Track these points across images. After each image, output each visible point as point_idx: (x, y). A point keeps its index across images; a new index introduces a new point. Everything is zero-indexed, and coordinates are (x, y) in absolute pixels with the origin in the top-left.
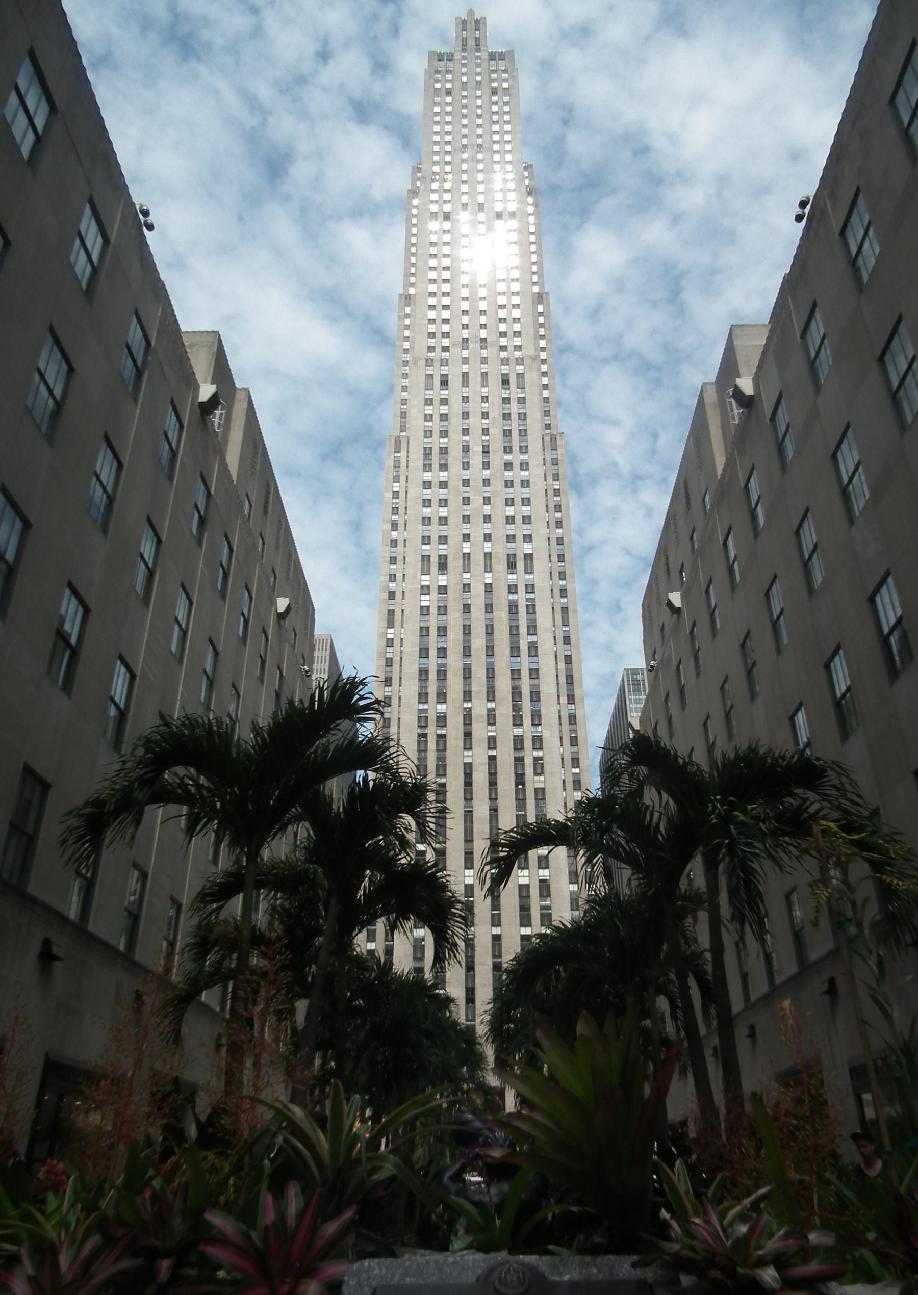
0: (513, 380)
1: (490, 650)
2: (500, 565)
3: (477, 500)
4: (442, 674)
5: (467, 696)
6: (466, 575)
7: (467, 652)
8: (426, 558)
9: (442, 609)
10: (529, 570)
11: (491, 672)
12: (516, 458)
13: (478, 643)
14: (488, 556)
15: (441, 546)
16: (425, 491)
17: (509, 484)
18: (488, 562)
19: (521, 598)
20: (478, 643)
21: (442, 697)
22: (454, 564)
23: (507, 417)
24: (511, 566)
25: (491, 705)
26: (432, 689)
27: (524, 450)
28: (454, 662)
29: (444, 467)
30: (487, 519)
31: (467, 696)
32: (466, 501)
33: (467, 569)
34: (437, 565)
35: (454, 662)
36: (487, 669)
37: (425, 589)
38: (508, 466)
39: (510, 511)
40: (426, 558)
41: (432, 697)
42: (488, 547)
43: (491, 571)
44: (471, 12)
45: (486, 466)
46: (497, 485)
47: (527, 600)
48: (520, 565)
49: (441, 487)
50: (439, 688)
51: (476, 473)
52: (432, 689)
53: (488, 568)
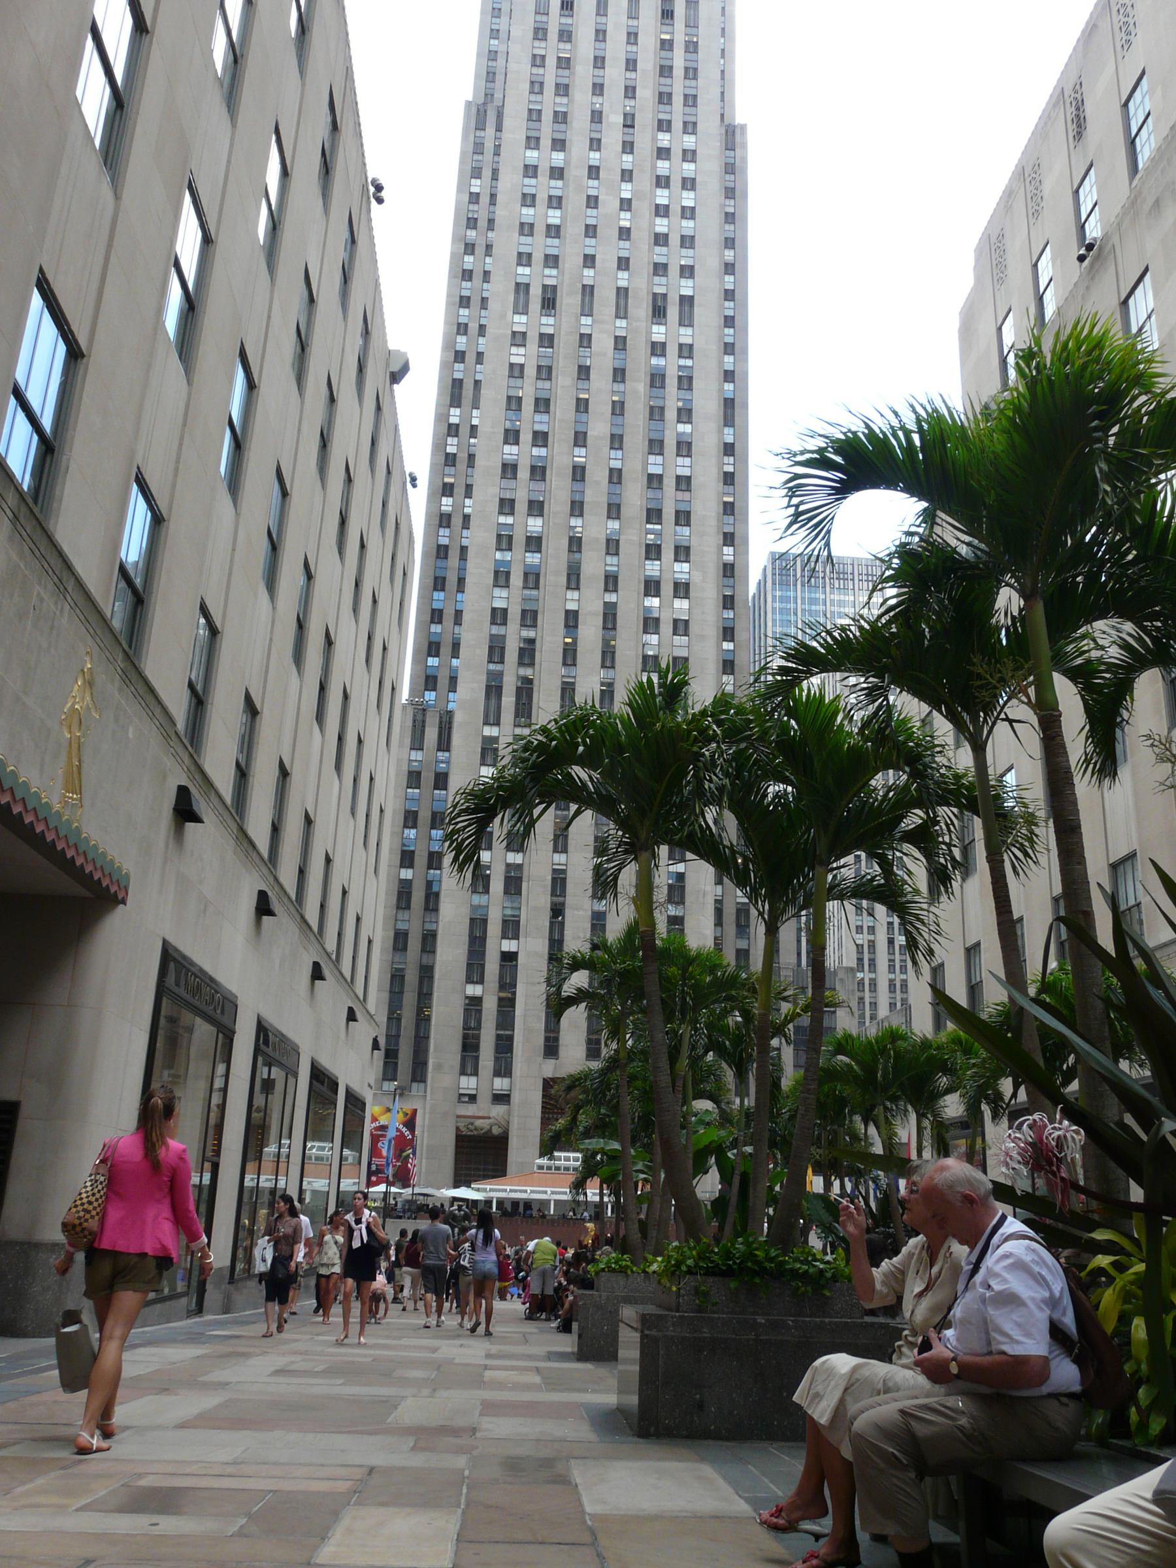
2: (640, 309)
3: (609, 203)
5: (577, 508)
8: (522, 289)
10: (686, 319)
14: (622, 293)
15: (547, 271)
16: (527, 181)
18: (622, 302)
19: (671, 364)
22: (569, 301)
24: (658, 311)
29: (559, 144)
30: (624, 234)
31: (577, 508)
32: (592, 202)
34: (539, 301)
38: (663, 153)
39: (661, 225)
40: (522, 289)
42: (623, 279)
43: (625, 318)
45: (628, 147)
48: (673, 312)
49: (552, 177)
51: (611, 157)
53: (621, 311)
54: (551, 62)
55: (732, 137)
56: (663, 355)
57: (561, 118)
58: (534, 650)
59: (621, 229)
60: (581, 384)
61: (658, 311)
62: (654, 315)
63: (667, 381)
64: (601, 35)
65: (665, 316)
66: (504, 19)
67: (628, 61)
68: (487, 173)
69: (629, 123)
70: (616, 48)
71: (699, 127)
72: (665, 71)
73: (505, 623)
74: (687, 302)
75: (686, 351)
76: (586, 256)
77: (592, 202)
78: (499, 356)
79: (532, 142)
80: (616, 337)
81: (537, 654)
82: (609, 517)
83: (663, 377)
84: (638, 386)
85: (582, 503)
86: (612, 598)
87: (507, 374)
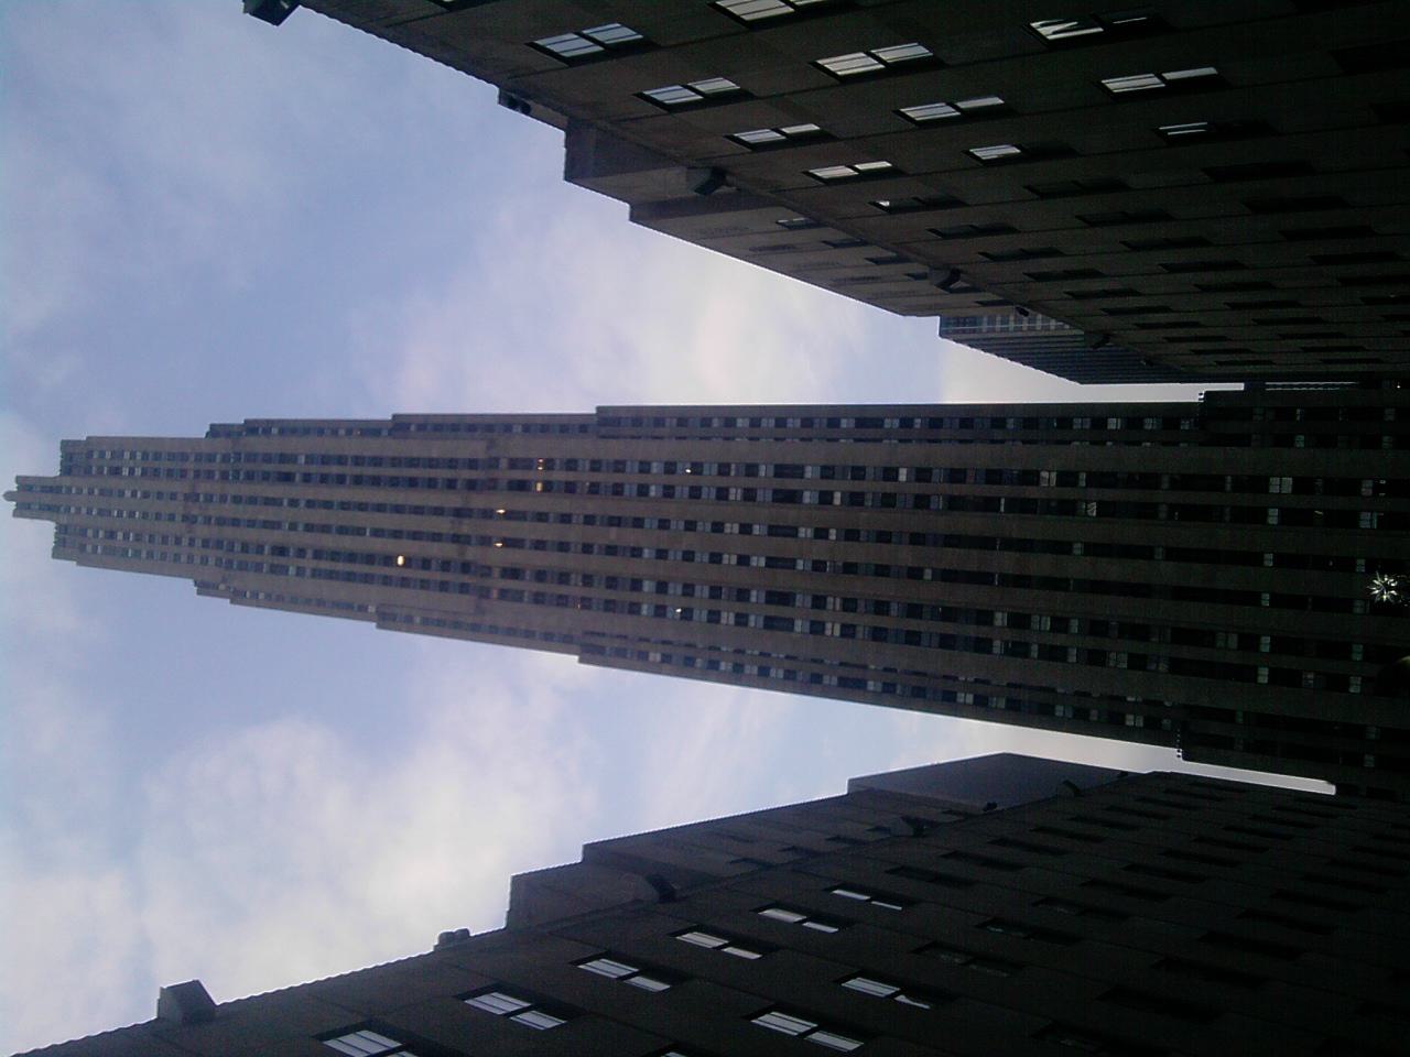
0: (518, 475)
2: (789, 514)
3: (689, 541)
6: (800, 565)
12: (631, 479)
14: (774, 531)
15: (830, 607)
17: (668, 492)
22: (781, 580)
23: (594, 489)
24: (791, 497)
26: (972, 630)
27: (619, 466)
33: (789, 564)
34: (781, 608)
38: (643, 491)
40: (770, 623)
41: (983, 631)
44: (9, 496)
45: (638, 523)
46: (670, 509)
47: (844, 478)
48: (791, 484)
52: (972, 630)
53: (791, 532)
57: (612, 582)
61: (791, 497)
63: (857, 490)
64: (540, 545)
65: (795, 492)
68: (643, 646)
69: (616, 522)
72: (570, 488)
74: (781, 471)
75: (827, 472)
77: (688, 556)
79: (634, 609)
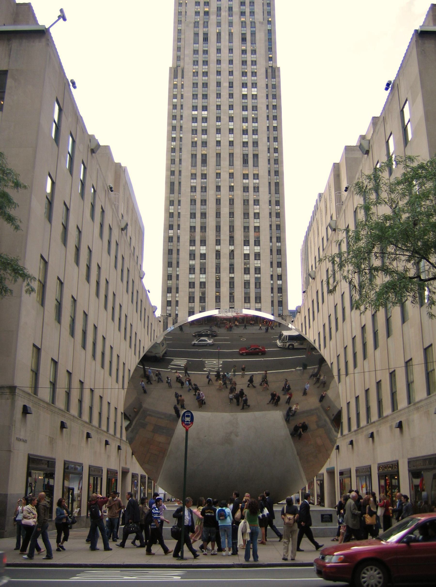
1: (232, 214)
4: (203, 228)
5: (218, 242)
7: (218, 215)
9: (204, 189)
10: (256, 164)
11: (232, 228)
13: (225, 210)
20: (225, 210)
21: (203, 242)
24: (245, 161)
25: (232, 248)
28: (211, 222)
30: (231, 131)
31: (218, 242)
34: (200, 161)
35: (211, 222)
36: (230, 226)
37: (194, 176)
40: (194, 156)
41: (198, 242)
50: (201, 237)
54: (201, 52)
55: (273, 72)
56: (248, 179)
58: (205, 297)
59: (230, 129)
60: (218, 193)
62: (243, 163)
66: (182, 61)
67: (229, 61)
69: (231, 85)
70: (225, 55)
71: (258, 85)
73: (194, 288)
76: (217, 105)
78: (187, 183)
80: (230, 173)
81: (206, 299)
82: (230, 245)
83: (248, 188)
84: (238, 194)
85: (220, 240)
86: (232, 275)
87: (190, 191)
